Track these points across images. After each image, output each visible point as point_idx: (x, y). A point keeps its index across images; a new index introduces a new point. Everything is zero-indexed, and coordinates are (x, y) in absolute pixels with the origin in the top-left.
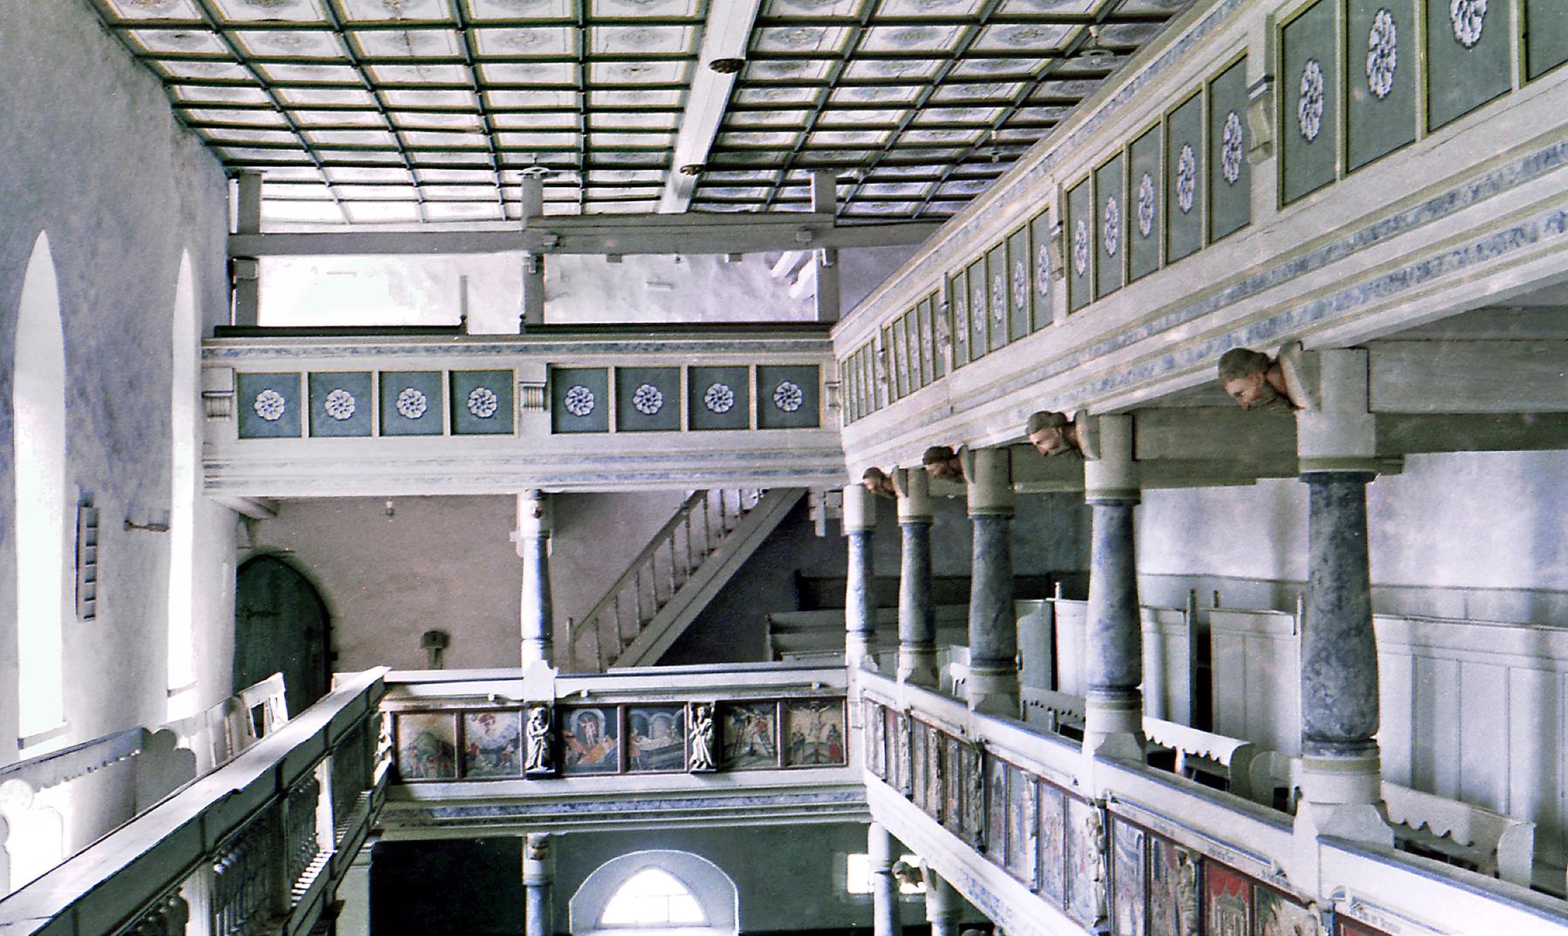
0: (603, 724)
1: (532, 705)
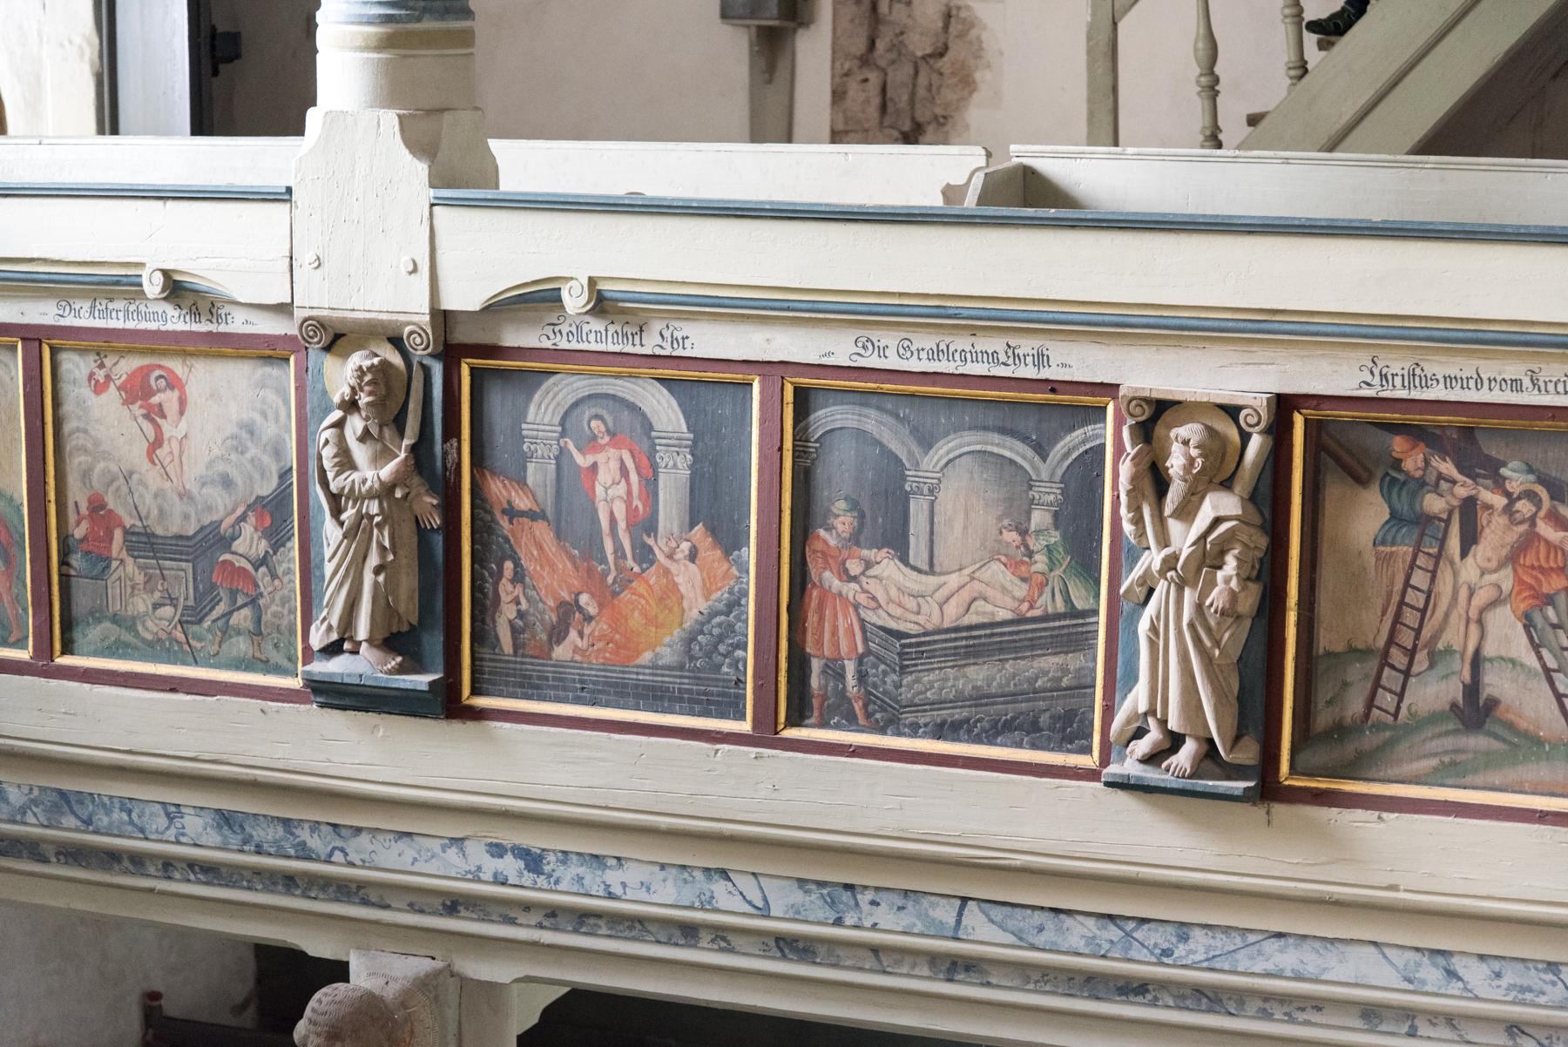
0: (675, 474)
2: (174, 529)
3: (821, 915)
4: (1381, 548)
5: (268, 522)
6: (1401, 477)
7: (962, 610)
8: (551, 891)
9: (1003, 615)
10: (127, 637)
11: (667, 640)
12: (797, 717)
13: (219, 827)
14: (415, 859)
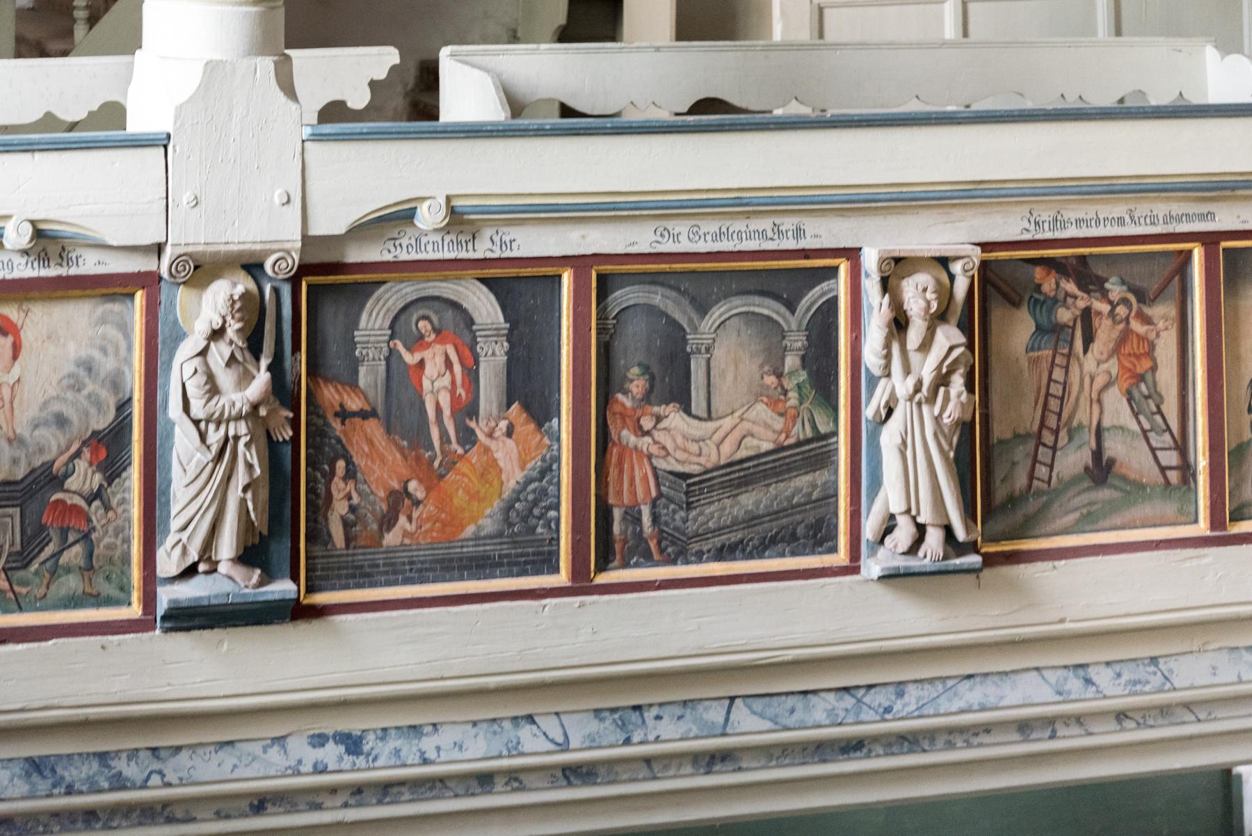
0: (493, 359)
1: (201, 270)
3: (612, 739)
4: (1031, 354)
5: (103, 454)
6: (1042, 298)
7: (735, 447)
8: (369, 769)
9: (766, 446)
11: (488, 511)
13: (28, 775)
14: (235, 766)
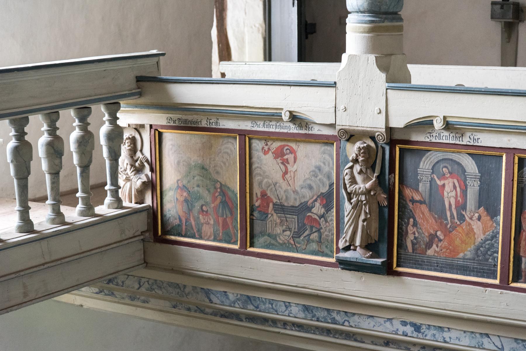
2: (291, 204)
5: (325, 202)
8: (423, 339)
10: (273, 242)
11: (469, 249)
12: (516, 279)
13: (304, 311)
14: (374, 326)
